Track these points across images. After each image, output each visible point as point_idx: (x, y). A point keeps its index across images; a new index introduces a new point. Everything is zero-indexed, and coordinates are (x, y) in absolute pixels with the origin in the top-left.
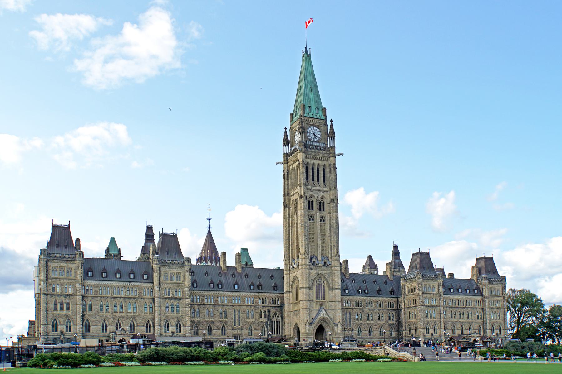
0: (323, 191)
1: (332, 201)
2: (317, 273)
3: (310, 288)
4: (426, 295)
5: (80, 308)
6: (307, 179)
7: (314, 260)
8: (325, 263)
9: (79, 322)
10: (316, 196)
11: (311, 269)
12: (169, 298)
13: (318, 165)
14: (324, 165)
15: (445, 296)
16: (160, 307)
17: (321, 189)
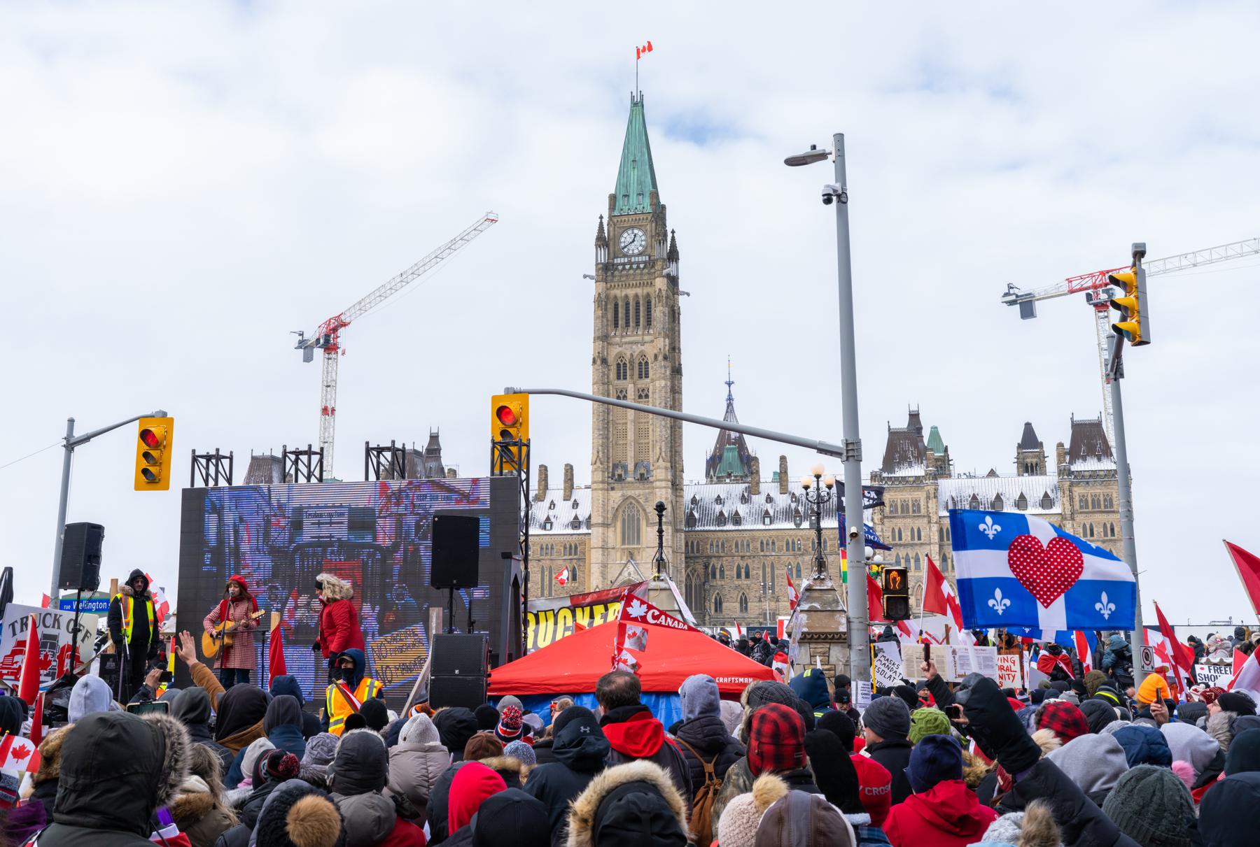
0: (643, 343)
1: (656, 357)
3: (605, 525)
4: (895, 521)
6: (616, 325)
7: (619, 471)
8: (642, 475)
10: (628, 357)
11: (613, 489)
13: (637, 296)
14: (648, 295)
17: (639, 338)
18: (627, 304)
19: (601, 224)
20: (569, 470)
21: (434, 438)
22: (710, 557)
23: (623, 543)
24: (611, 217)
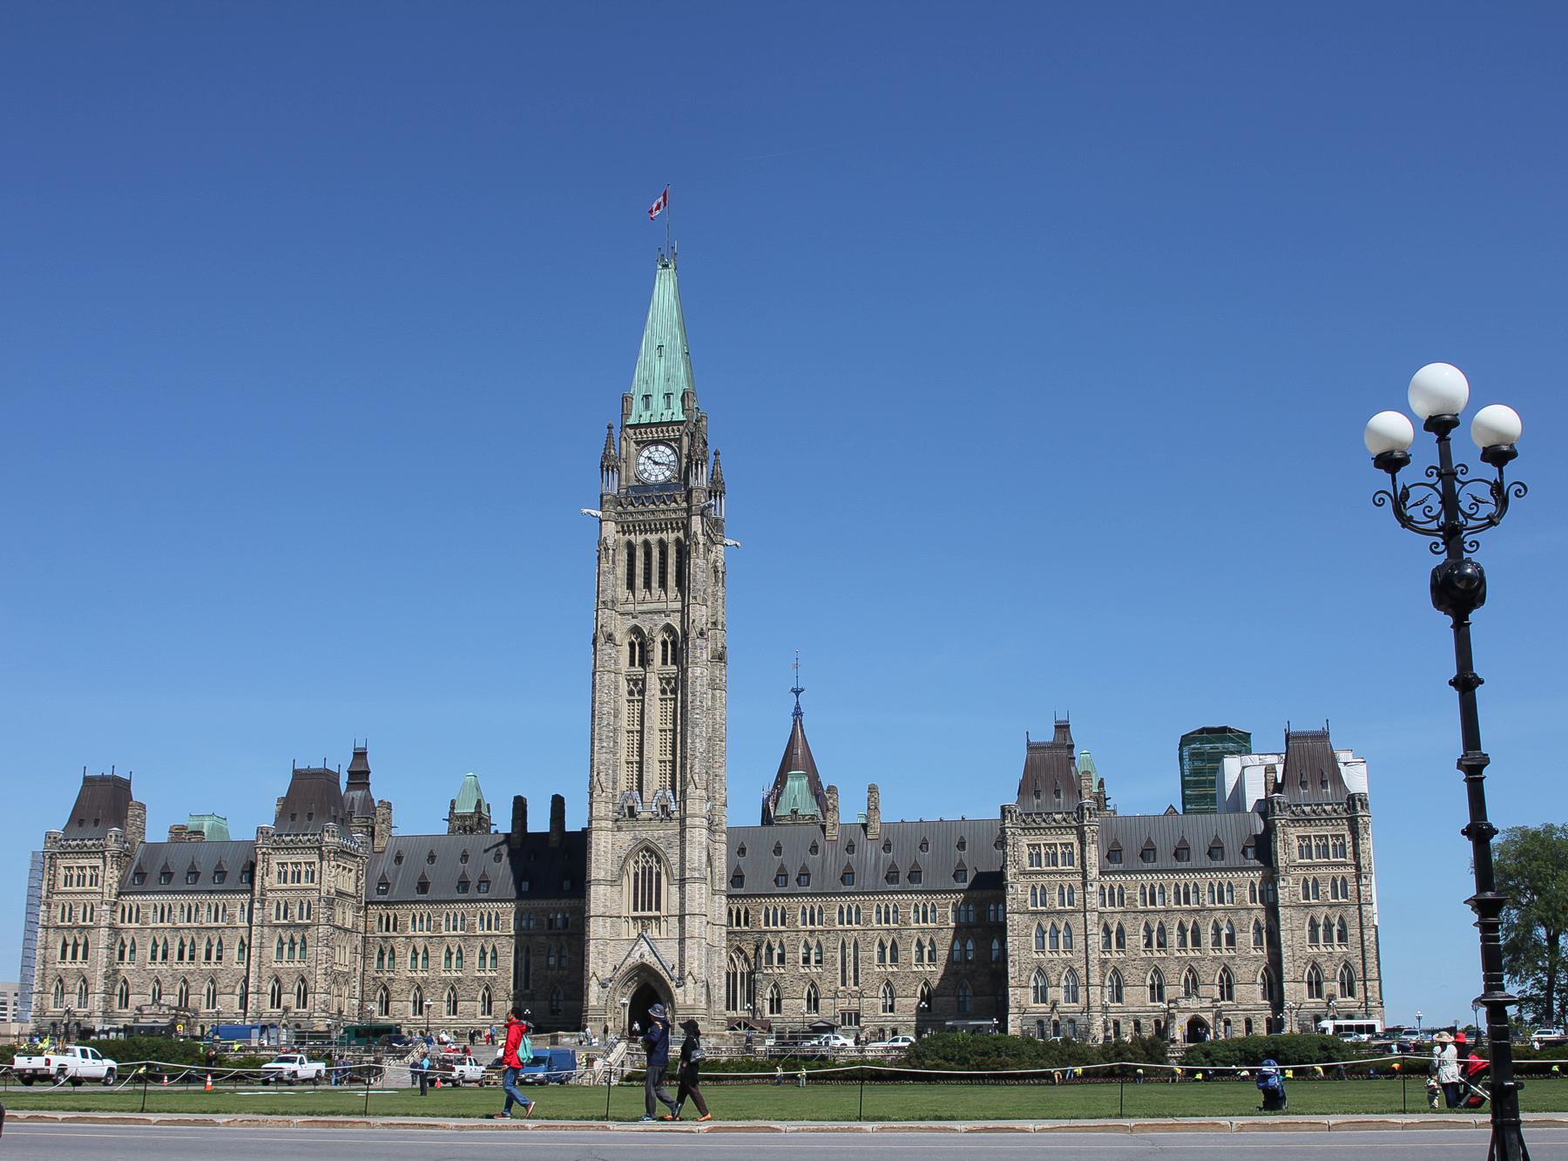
2: (635, 838)
5: (100, 955)
9: (98, 985)
11: (619, 829)
12: (283, 926)
14: (678, 540)
15: (1118, 879)
16: (261, 946)
17: (662, 606)
18: (648, 555)
19: (610, 435)
20: (558, 804)
21: (360, 755)
22: (766, 932)
23: (636, 909)
24: (624, 427)
